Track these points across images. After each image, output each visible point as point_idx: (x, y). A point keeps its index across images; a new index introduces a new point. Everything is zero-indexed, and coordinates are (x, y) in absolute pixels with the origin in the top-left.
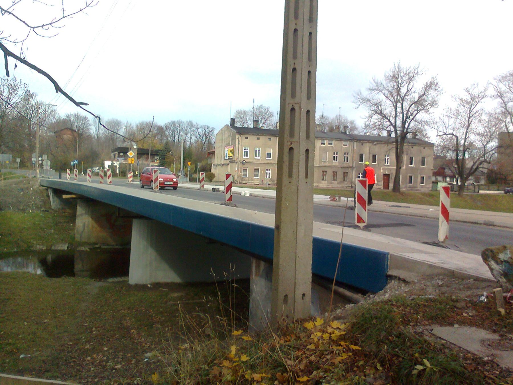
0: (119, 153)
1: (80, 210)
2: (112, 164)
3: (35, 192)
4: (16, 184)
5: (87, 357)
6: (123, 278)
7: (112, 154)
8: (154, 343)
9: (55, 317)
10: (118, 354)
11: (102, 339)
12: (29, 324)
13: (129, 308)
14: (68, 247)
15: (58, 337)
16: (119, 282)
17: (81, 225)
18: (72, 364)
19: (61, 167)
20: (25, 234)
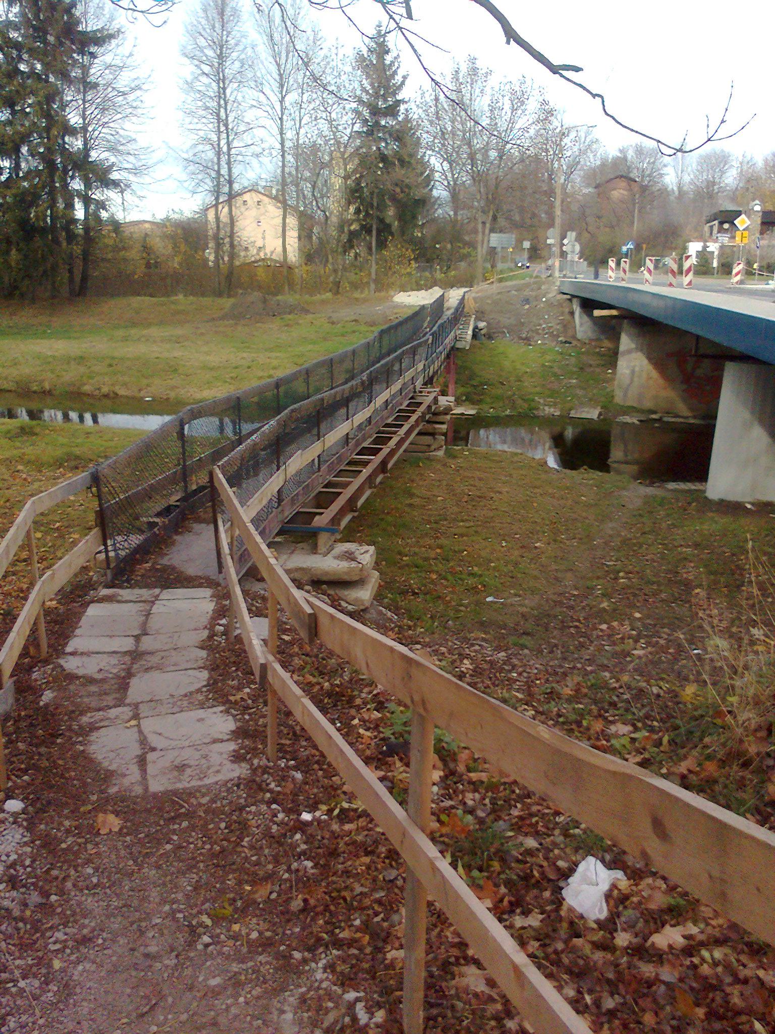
0: (721, 223)
1: (626, 342)
2: (705, 247)
3: (549, 304)
4: (519, 289)
5: (600, 623)
6: (697, 484)
7: (706, 228)
8: (737, 622)
9: (555, 541)
10: (661, 630)
11: (635, 595)
12: (510, 545)
13: (696, 545)
14: (600, 414)
15: (556, 579)
16: (683, 491)
17: (627, 372)
18: (572, 630)
19: (598, 258)
20: (526, 384)
